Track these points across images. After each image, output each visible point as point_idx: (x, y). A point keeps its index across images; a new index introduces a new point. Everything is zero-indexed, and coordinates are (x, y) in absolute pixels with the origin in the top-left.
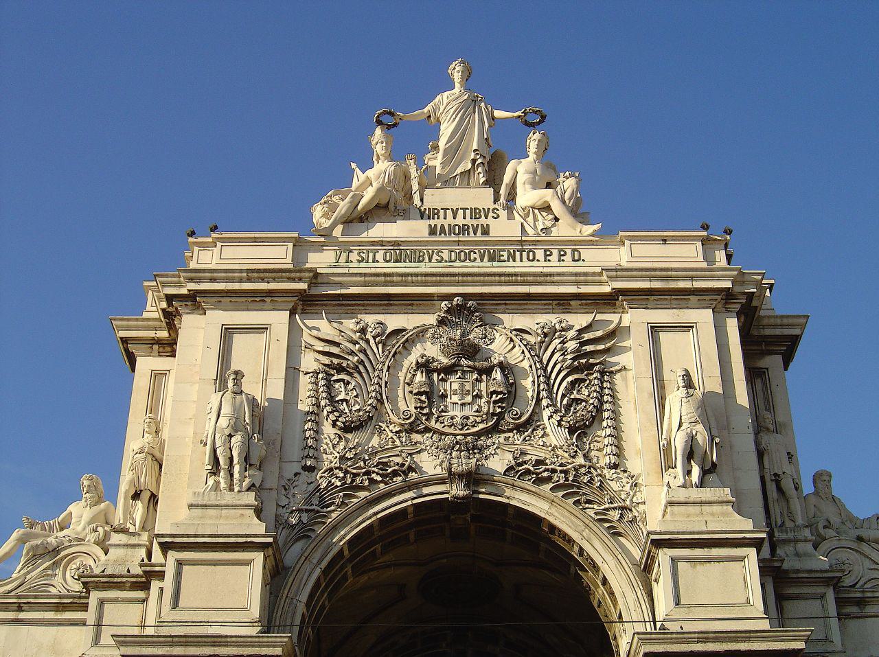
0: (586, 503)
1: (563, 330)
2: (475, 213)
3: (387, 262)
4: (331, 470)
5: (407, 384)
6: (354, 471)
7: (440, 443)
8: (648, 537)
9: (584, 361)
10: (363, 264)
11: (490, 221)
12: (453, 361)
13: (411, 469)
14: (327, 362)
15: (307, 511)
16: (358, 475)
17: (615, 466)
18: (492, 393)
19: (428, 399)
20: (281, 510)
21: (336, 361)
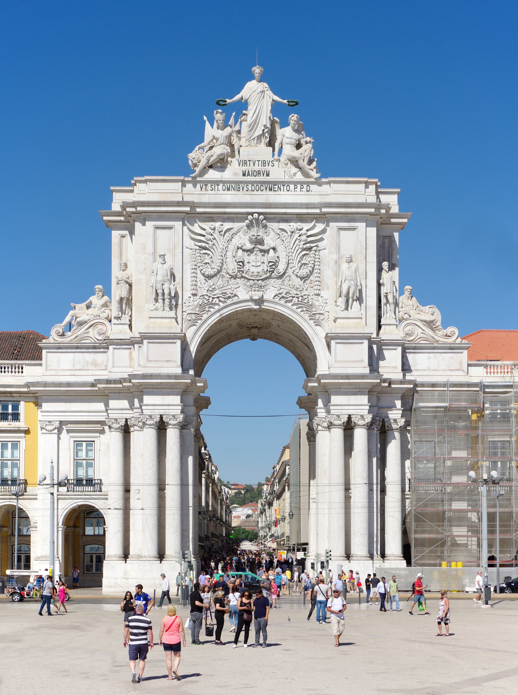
0: (306, 310)
1: (301, 230)
2: (264, 163)
3: (224, 190)
4: (204, 295)
5: (234, 257)
6: (213, 296)
7: (248, 284)
8: (327, 334)
9: (308, 245)
10: (213, 192)
11: (269, 168)
12: (253, 246)
13: (235, 295)
14: (200, 244)
15: (194, 314)
16: (215, 298)
17: (318, 295)
18: (269, 262)
19: (243, 264)
20: (184, 313)
21: (204, 245)
